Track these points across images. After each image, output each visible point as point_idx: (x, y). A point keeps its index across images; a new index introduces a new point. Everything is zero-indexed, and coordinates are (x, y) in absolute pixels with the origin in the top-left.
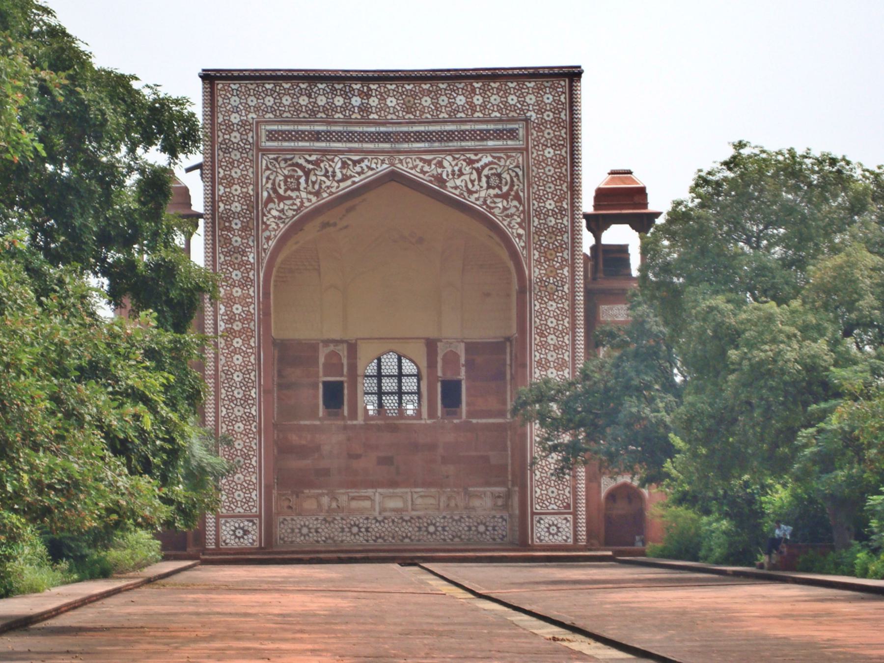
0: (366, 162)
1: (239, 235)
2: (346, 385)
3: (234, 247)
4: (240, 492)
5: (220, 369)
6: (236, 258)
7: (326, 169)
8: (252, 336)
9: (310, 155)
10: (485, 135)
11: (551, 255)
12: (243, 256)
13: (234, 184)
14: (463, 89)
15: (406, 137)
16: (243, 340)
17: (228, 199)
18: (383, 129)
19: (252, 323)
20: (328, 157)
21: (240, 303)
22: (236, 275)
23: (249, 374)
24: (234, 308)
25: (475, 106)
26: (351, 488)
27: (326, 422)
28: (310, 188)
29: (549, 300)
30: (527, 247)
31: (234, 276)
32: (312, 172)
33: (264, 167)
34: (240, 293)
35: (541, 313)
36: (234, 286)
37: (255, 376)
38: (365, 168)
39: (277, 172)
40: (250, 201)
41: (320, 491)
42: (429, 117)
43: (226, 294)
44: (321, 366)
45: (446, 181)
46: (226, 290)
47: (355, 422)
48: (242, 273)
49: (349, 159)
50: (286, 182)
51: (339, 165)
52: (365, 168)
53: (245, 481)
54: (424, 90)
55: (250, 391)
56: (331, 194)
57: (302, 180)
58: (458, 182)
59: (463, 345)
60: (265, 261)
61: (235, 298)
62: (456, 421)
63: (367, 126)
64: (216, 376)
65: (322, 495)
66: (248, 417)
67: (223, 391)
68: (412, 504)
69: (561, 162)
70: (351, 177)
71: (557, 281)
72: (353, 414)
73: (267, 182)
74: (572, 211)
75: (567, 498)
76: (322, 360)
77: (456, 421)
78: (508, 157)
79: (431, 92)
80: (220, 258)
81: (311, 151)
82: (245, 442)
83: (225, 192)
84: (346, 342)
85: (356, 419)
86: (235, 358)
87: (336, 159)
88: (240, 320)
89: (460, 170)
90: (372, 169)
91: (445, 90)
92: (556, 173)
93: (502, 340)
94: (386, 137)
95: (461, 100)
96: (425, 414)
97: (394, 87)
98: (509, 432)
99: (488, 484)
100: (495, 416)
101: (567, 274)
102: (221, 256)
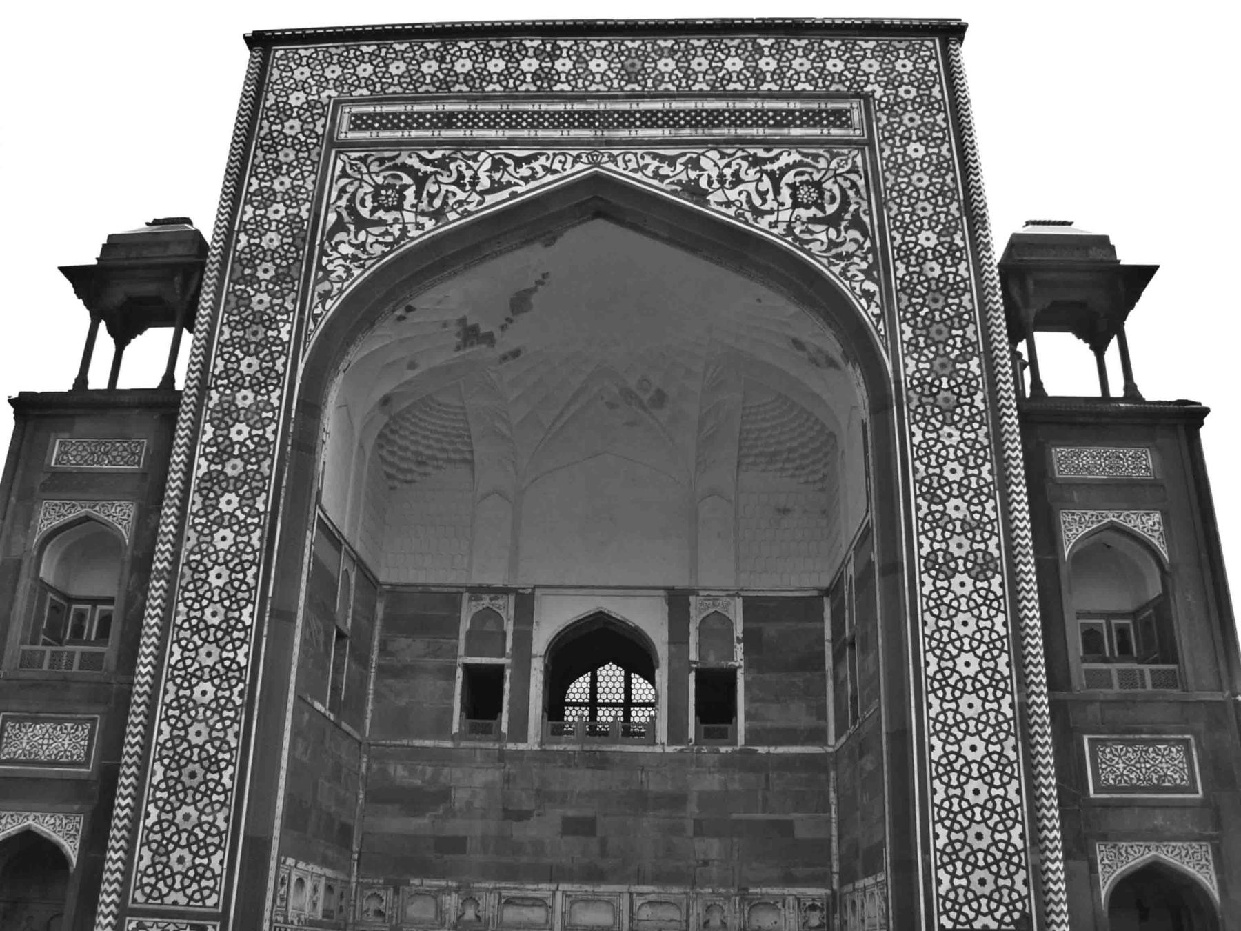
0: (542, 160)
1: (268, 291)
2: (508, 672)
3: (254, 313)
4: (185, 852)
5: (183, 560)
6: (255, 333)
7: (459, 172)
8: (262, 490)
9: (431, 152)
10: (784, 119)
11: (939, 332)
12: (269, 328)
13: (275, 201)
14: (738, 48)
15: (627, 120)
16: (242, 497)
17: (259, 227)
18: (578, 106)
19: (268, 461)
20: (466, 153)
21: (247, 421)
22: (249, 365)
23: (244, 571)
24: (233, 430)
25: (764, 73)
26: (506, 879)
27: (463, 744)
28: (424, 206)
29: (944, 423)
30: (886, 314)
31: (243, 368)
32: (432, 178)
33: (337, 173)
34: (250, 401)
35: (928, 451)
36: (242, 387)
37: (256, 576)
38: (539, 169)
39: (361, 180)
40: (301, 229)
41: (443, 883)
42: (670, 86)
43: (220, 403)
44: (462, 637)
45: (706, 193)
46: (222, 394)
47: (521, 746)
48: (262, 360)
49: (508, 156)
50: (376, 195)
51: (488, 164)
52: (539, 169)
53: (200, 824)
54: (661, 48)
55: (240, 609)
56: (467, 213)
57: (410, 193)
58: (733, 195)
59: (739, 601)
60: (313, 339)
61: (238, 410)
62: (723, 750)
63: (548, 103)
64: (172, 575)
65: (446, 891)
66: (228, 669)
67: (181, 607)
68: (631, 919)
69: (941, 167)
70: (509, 184)
71: (958, 385)
72: (519, 732)
73: (339, 197)
74: (976, 254)
75: (1021, 899)
76: (465, 625)
77: (723, 750)
78: (833, 156)
79: (676, 52)
80: (221, 333)
81: (431, 145)
82: (212, 728)
83: (255, 216)
84: (514, 591)
85: (525, 740)
86: (217, 536)
87: (483, 156)
88: (241, 455)
89: (736, 174)
90: (556, 172)
91: (704, 48)
92: (932, 184)
93: (815, 593)
94: (586, 120)
95: (734, 64)
96: (662, 734)
97: (603, 44)
98: (832, 774)
99: (789, 880)
100: (803, 744)
101: (978, 372)
102: (225, 329)
